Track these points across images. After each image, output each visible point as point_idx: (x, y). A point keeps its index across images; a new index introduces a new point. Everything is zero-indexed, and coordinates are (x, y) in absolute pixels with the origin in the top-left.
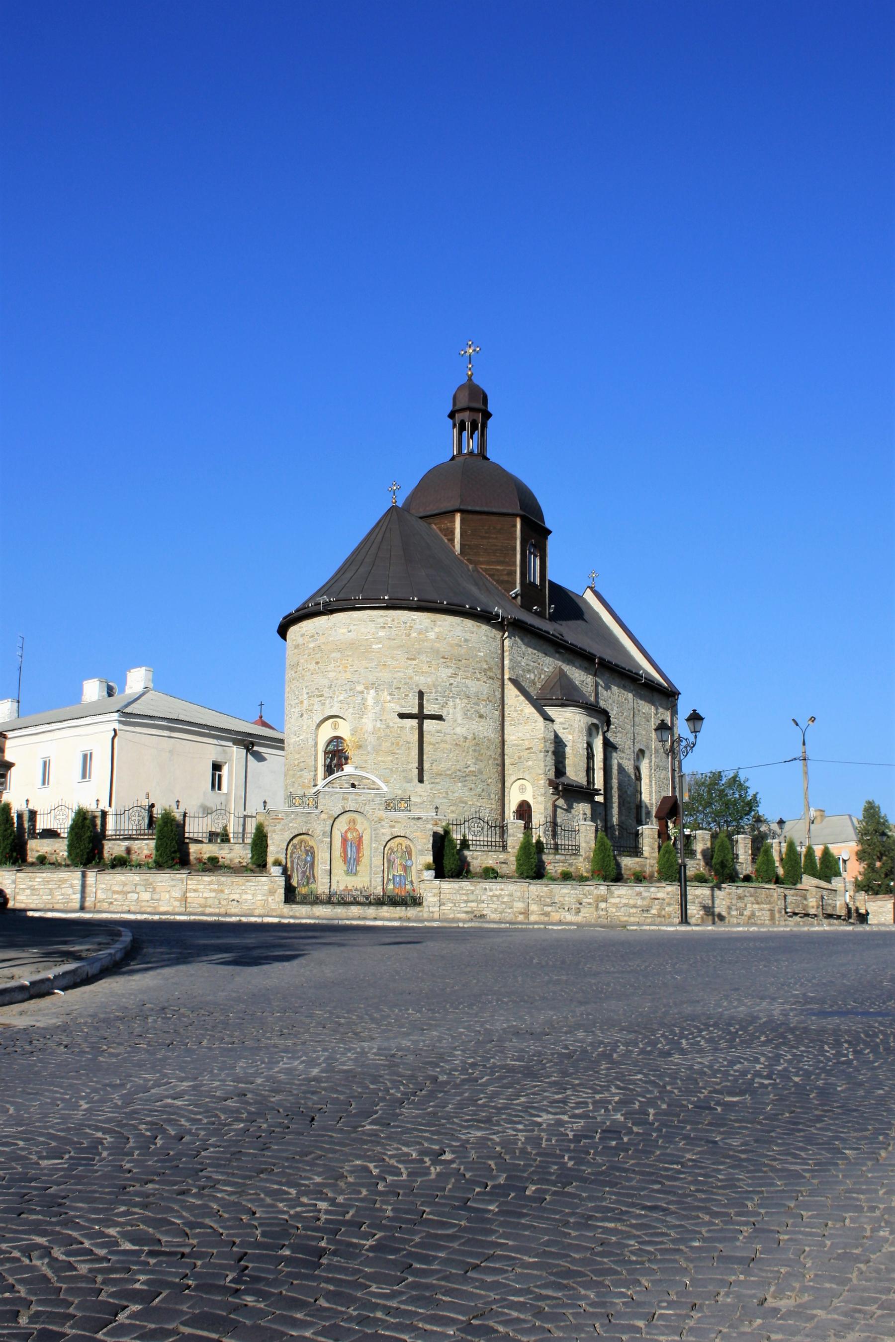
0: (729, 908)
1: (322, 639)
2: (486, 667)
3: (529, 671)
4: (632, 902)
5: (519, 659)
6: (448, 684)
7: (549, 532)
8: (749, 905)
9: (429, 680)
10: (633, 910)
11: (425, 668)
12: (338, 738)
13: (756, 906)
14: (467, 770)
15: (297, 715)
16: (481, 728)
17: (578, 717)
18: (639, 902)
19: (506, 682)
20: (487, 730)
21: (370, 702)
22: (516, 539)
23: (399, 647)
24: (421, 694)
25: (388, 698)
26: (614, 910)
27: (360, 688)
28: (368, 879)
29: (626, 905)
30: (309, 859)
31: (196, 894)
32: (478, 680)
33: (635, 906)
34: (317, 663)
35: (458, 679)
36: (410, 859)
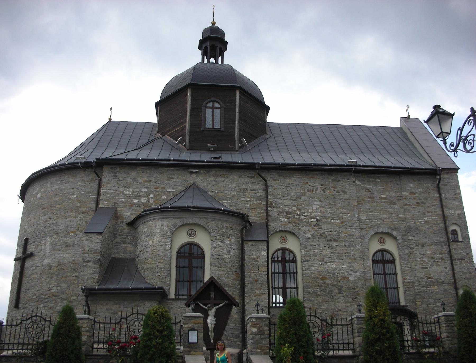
2: (78, 205)
3: (139, 197)
5: (121, 189)
6: (43, 227)
9: (33, 228)
11: (33, 221)
14: (49, 292)
16: (67, 255)
17: (159, 223)
22: (186, 103)
24: (27, 241)
32: (70, 216)
35: (51, 220)
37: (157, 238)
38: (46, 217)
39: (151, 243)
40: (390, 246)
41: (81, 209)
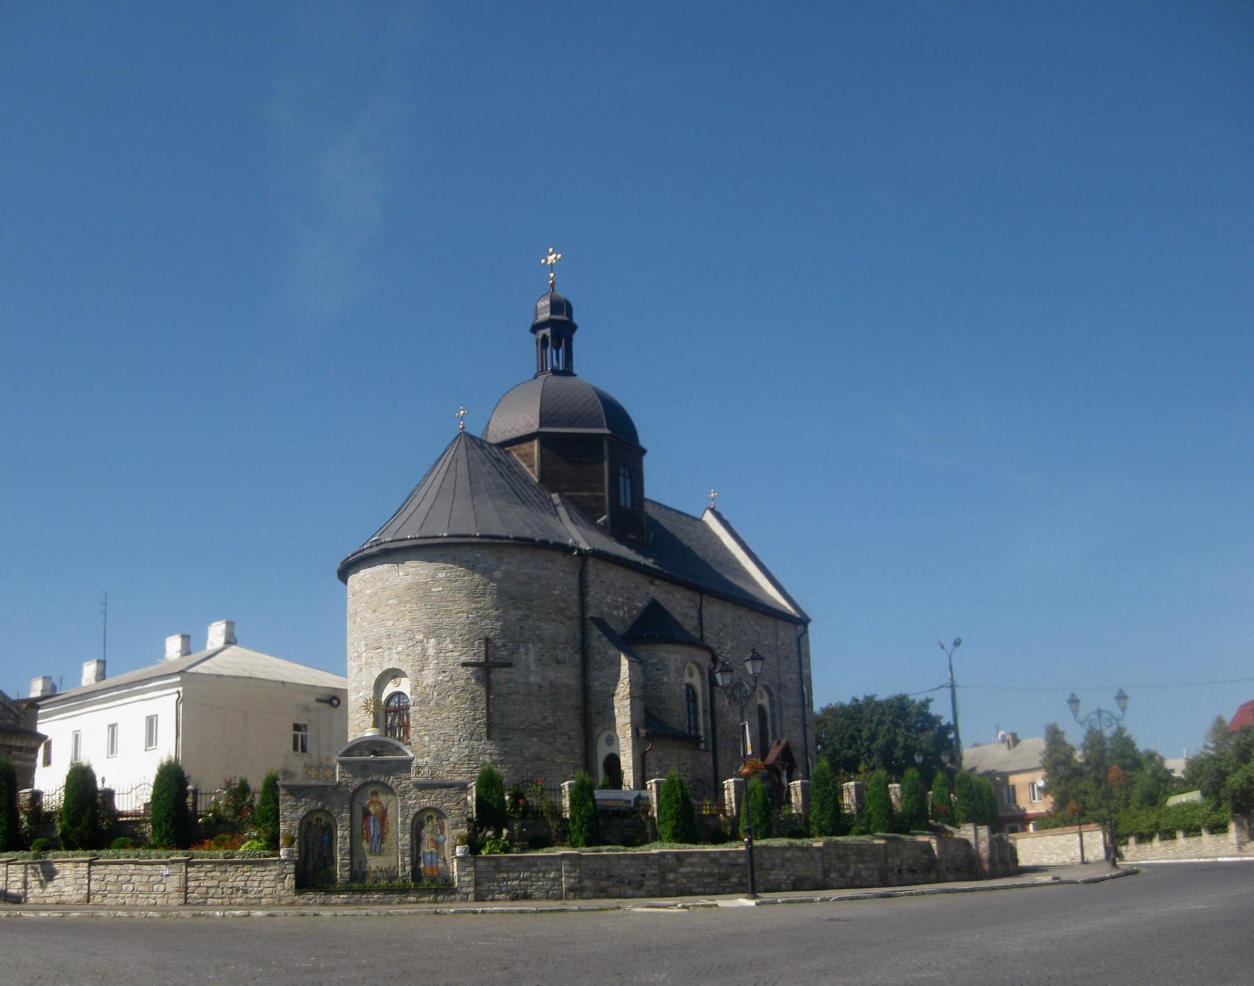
0: (826, 872)
1: (379, 585)
3: (617, 608)
4: (706, 870)
7: (643, 452)
8: (852, 866)
10: (709, 880)
12: (399, 694)
13: (861, 866)
15: (356, 670)
17: (673, 657)
18: (716, 870)
19: (589, 622)
20: (567, 677)
21: (431, 652)
23: (460, 590)
25: (451, 646)
26: (685, 881)
27: (420, 637)
28: (393, 857)
29: (699, 875)
30: (326, 837)
31: (196, 883)
32: (554, 620)
33: (710, 875)
34: (374, 611)
35: (530, 621)
36: (442, 833)
37: (673, 676)
38: (520, 612)
39: (666, 679)
40: (765, 701)
41: (567, 613)
